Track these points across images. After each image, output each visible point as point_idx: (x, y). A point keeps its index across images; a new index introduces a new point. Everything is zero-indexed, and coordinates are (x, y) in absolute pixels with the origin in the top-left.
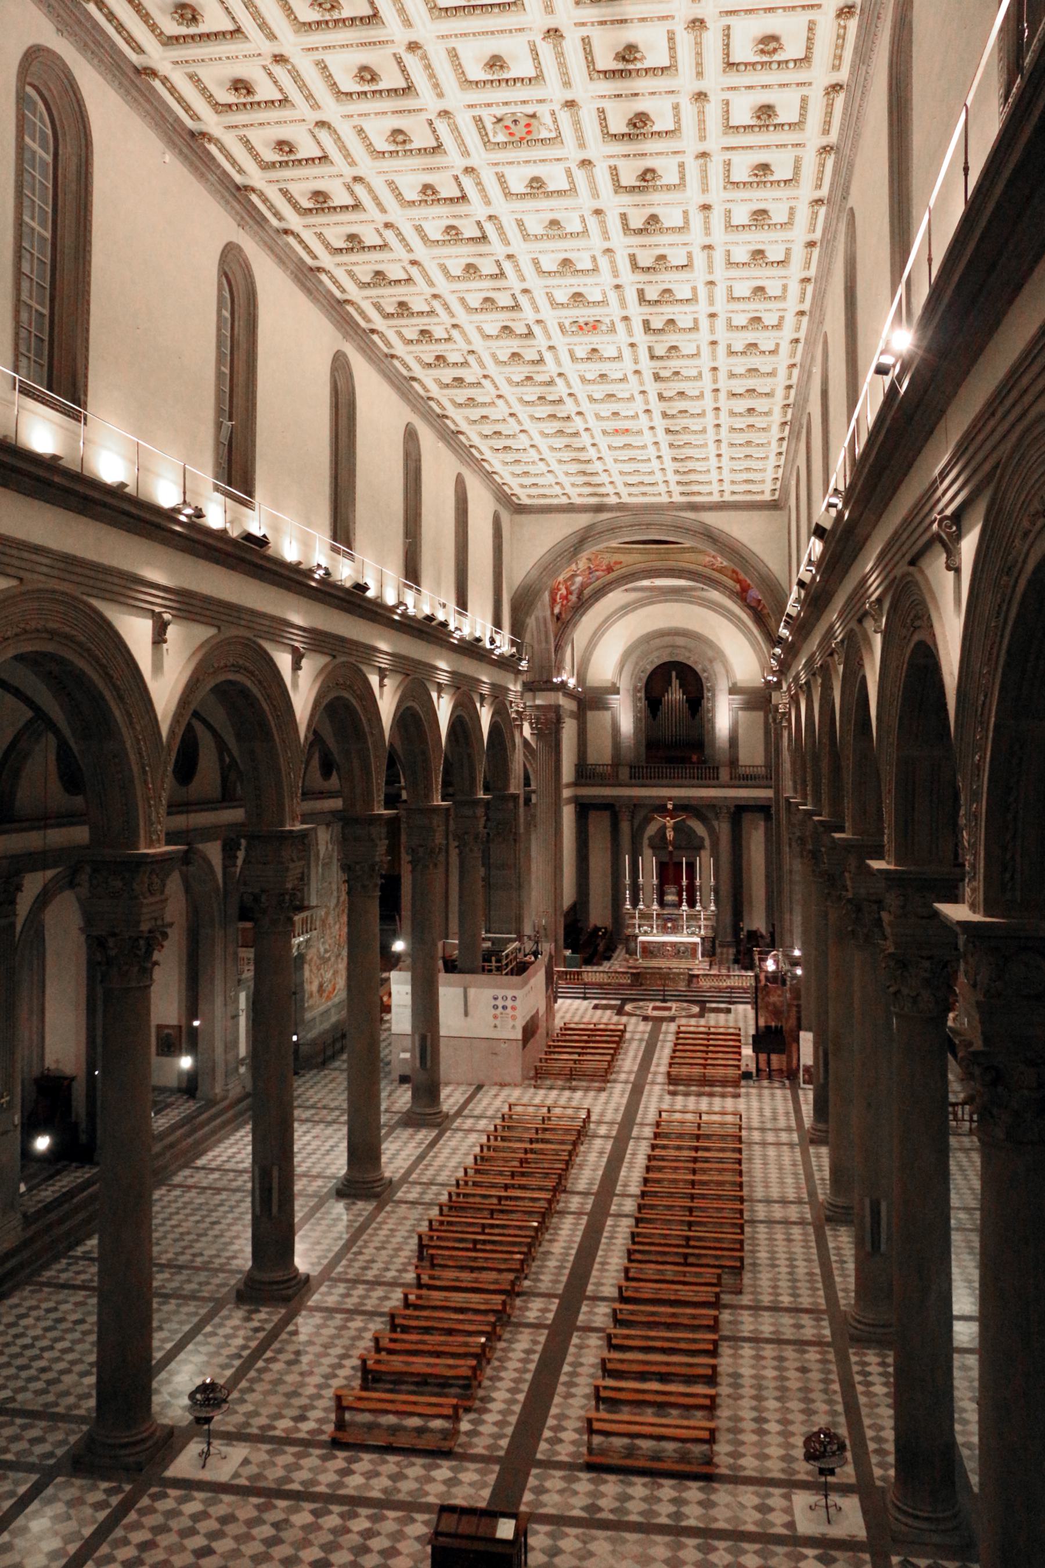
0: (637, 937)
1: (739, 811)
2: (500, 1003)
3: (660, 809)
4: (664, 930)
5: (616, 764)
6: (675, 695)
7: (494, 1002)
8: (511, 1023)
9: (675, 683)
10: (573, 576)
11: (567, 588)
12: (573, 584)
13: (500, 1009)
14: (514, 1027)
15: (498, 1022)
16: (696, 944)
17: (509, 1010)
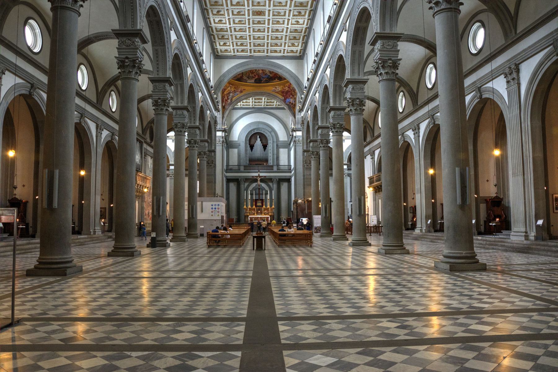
0: (248, 216)
1: (281, 181)
2: (214, 207)
3: (254, 180)
4: (257, 213)
5: (239, 165)
6: (258, 143)
7: (212, 207)
8: (218, 214)
9: (259, 139)
10: (230, 93)
11: (227, 97)
12: (229, 96)
13: (214, 209)
14: (218, 215)
15: (213, 214)
16: (268, 217)
17: (217, 209)
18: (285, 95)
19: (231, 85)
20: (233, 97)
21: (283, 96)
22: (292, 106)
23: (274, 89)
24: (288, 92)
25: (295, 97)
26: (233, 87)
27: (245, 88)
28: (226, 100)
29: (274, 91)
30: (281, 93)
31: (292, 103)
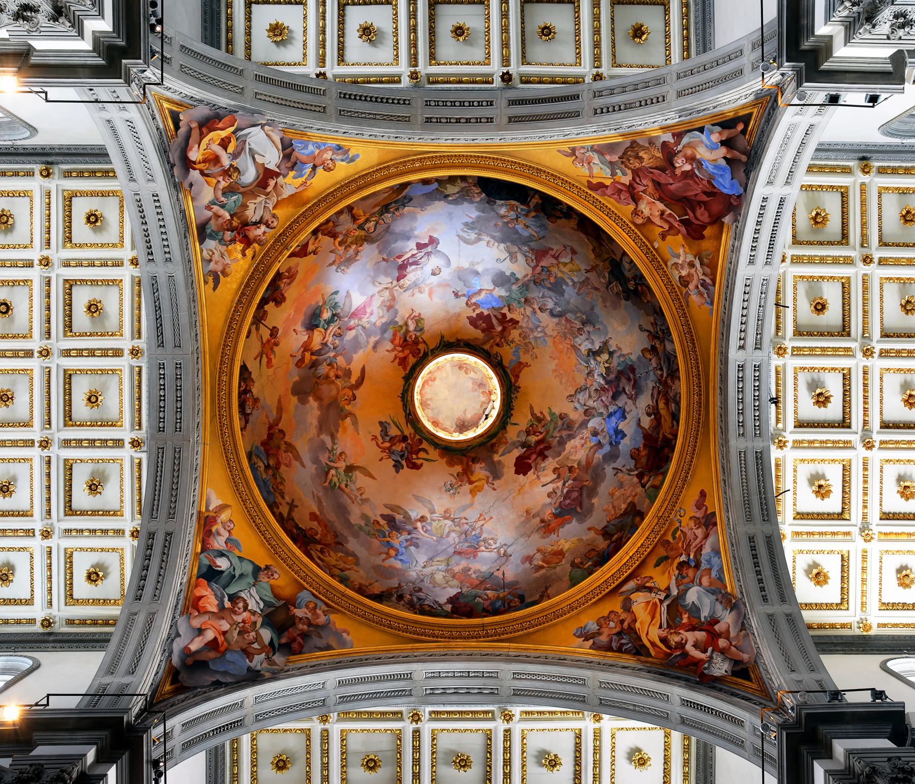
10: (676, 606)
11: (693, 628)
12: (695, 610)
18: (702, 215)
19: (631, 584)
20: (718, 591)
21: (717, 221)
22: (742, 142)
23: (694, 298)
24: (663, 193)
25: (668, 137)
26: (650, 571)
27: (690, 497)
28: (714, 636)
29: (706, 287)
30: (706, 245)
31: (723, 143)
